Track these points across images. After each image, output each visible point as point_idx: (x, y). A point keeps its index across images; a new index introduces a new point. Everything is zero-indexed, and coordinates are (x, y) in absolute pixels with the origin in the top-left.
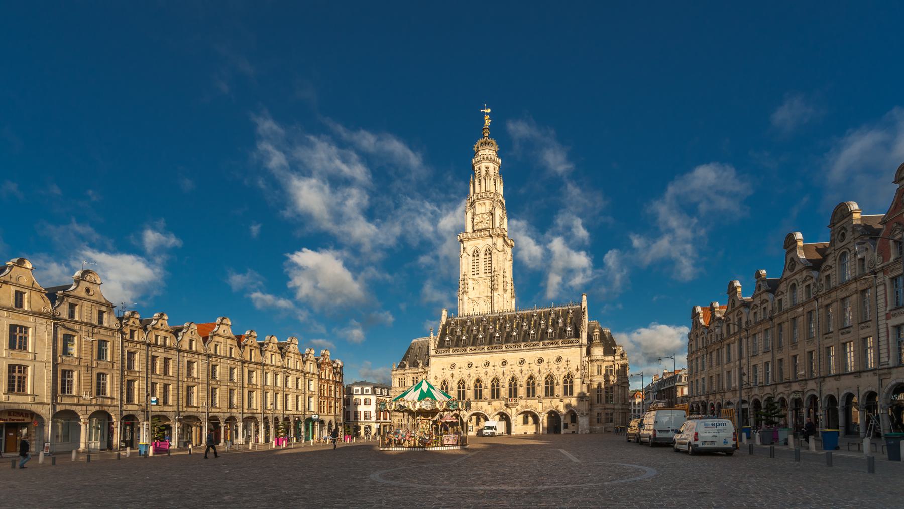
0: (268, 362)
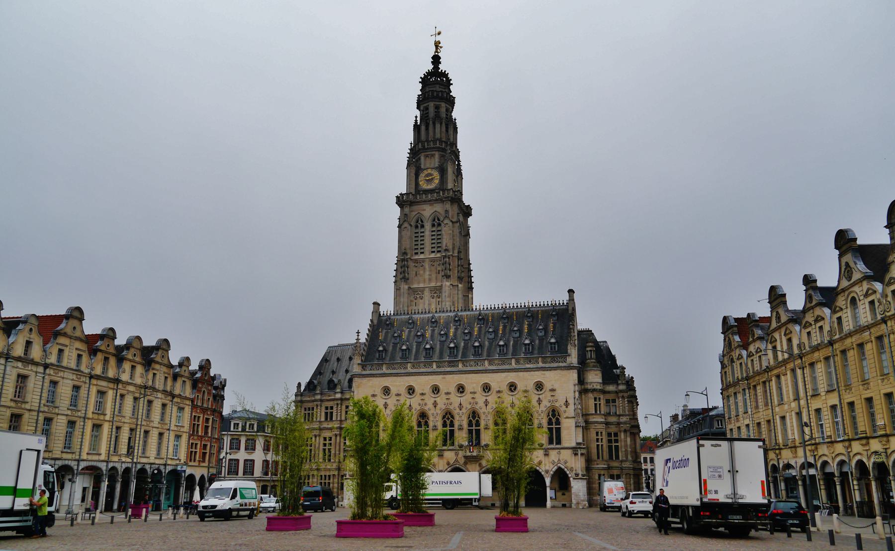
0: (125, 377)
